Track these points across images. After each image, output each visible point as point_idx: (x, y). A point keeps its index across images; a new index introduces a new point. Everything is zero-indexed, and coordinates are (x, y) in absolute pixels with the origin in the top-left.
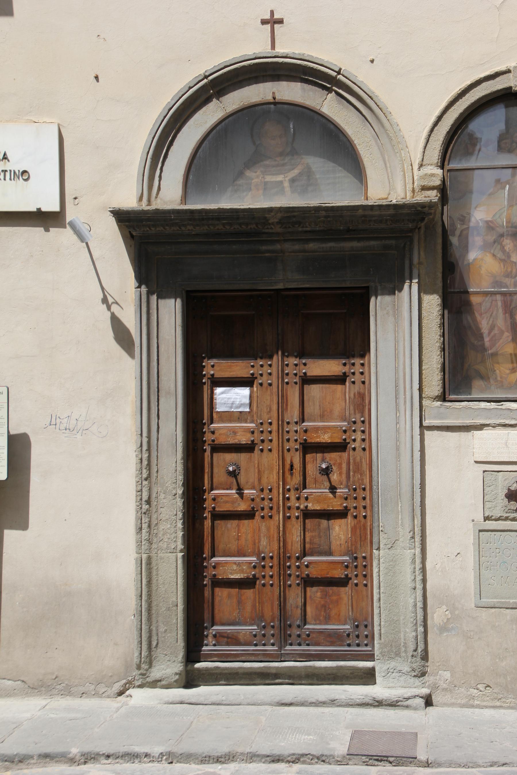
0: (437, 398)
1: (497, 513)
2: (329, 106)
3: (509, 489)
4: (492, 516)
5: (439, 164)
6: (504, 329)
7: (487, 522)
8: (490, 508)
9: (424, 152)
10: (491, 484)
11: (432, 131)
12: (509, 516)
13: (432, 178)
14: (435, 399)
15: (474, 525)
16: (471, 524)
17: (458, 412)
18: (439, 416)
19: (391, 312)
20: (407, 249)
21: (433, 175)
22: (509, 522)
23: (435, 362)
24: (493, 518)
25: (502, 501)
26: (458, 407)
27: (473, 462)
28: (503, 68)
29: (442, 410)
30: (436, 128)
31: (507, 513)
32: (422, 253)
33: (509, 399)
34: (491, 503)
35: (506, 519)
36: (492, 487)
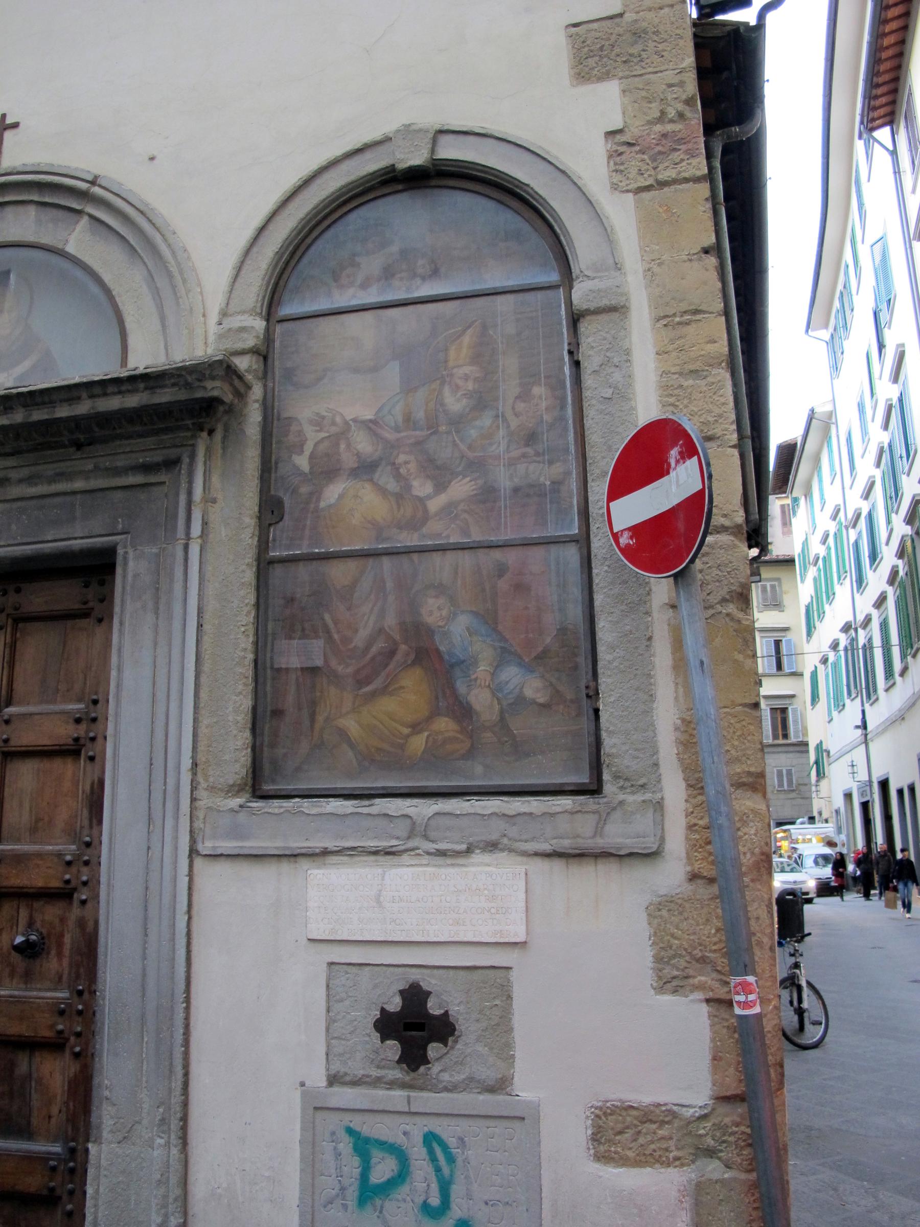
0: (235, 790)
1: (357, 1067)
2: (78, 240)
3: (383, 1010)
4: (346, 1074)
5: (258, 310)
6: (397, 637)
7: (336, 1089)
8: (341, 1055)
9: (231, 292)
10: (344, 995)
11: (247, 252)
12: (383, 1077)
13: (242, 335)
14: (228, 792)
15: (304, 1095)
16: (297, 1095)
17: (276, 826)
18: (236, 832)
19: (150, 605)
20: (183, 472)
21: (243, 329)
22: (381, 1093)
23: (231, 709)
24: (348, 1079)
25: (367, 1039)
26: (276, 811)
27: (305, 941)
28: (377, 135)
29: (242, 817)
30: (255, 249)
31: (378, 1067)
32: (215, 479)
33: (390, 791)
34: (343, 1042)
35: (376, 1082)
36: (347, 1003)
